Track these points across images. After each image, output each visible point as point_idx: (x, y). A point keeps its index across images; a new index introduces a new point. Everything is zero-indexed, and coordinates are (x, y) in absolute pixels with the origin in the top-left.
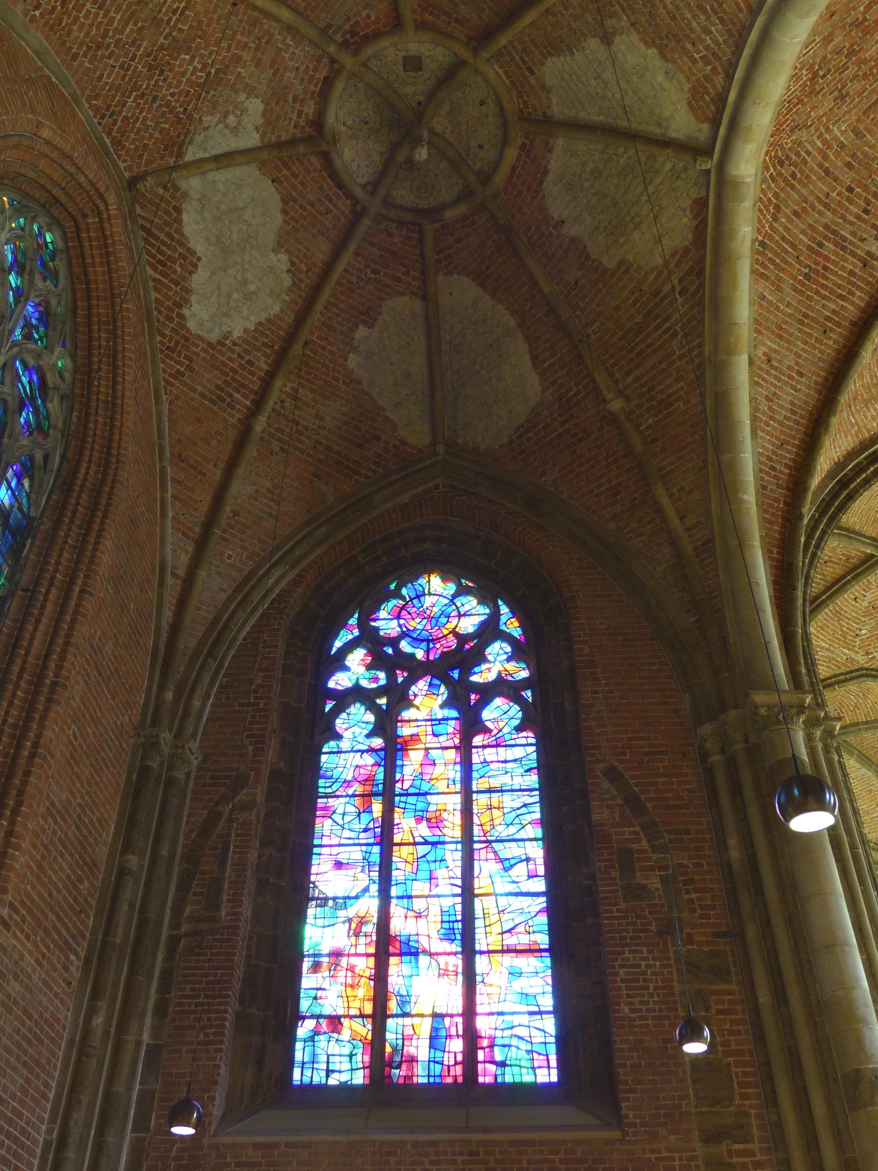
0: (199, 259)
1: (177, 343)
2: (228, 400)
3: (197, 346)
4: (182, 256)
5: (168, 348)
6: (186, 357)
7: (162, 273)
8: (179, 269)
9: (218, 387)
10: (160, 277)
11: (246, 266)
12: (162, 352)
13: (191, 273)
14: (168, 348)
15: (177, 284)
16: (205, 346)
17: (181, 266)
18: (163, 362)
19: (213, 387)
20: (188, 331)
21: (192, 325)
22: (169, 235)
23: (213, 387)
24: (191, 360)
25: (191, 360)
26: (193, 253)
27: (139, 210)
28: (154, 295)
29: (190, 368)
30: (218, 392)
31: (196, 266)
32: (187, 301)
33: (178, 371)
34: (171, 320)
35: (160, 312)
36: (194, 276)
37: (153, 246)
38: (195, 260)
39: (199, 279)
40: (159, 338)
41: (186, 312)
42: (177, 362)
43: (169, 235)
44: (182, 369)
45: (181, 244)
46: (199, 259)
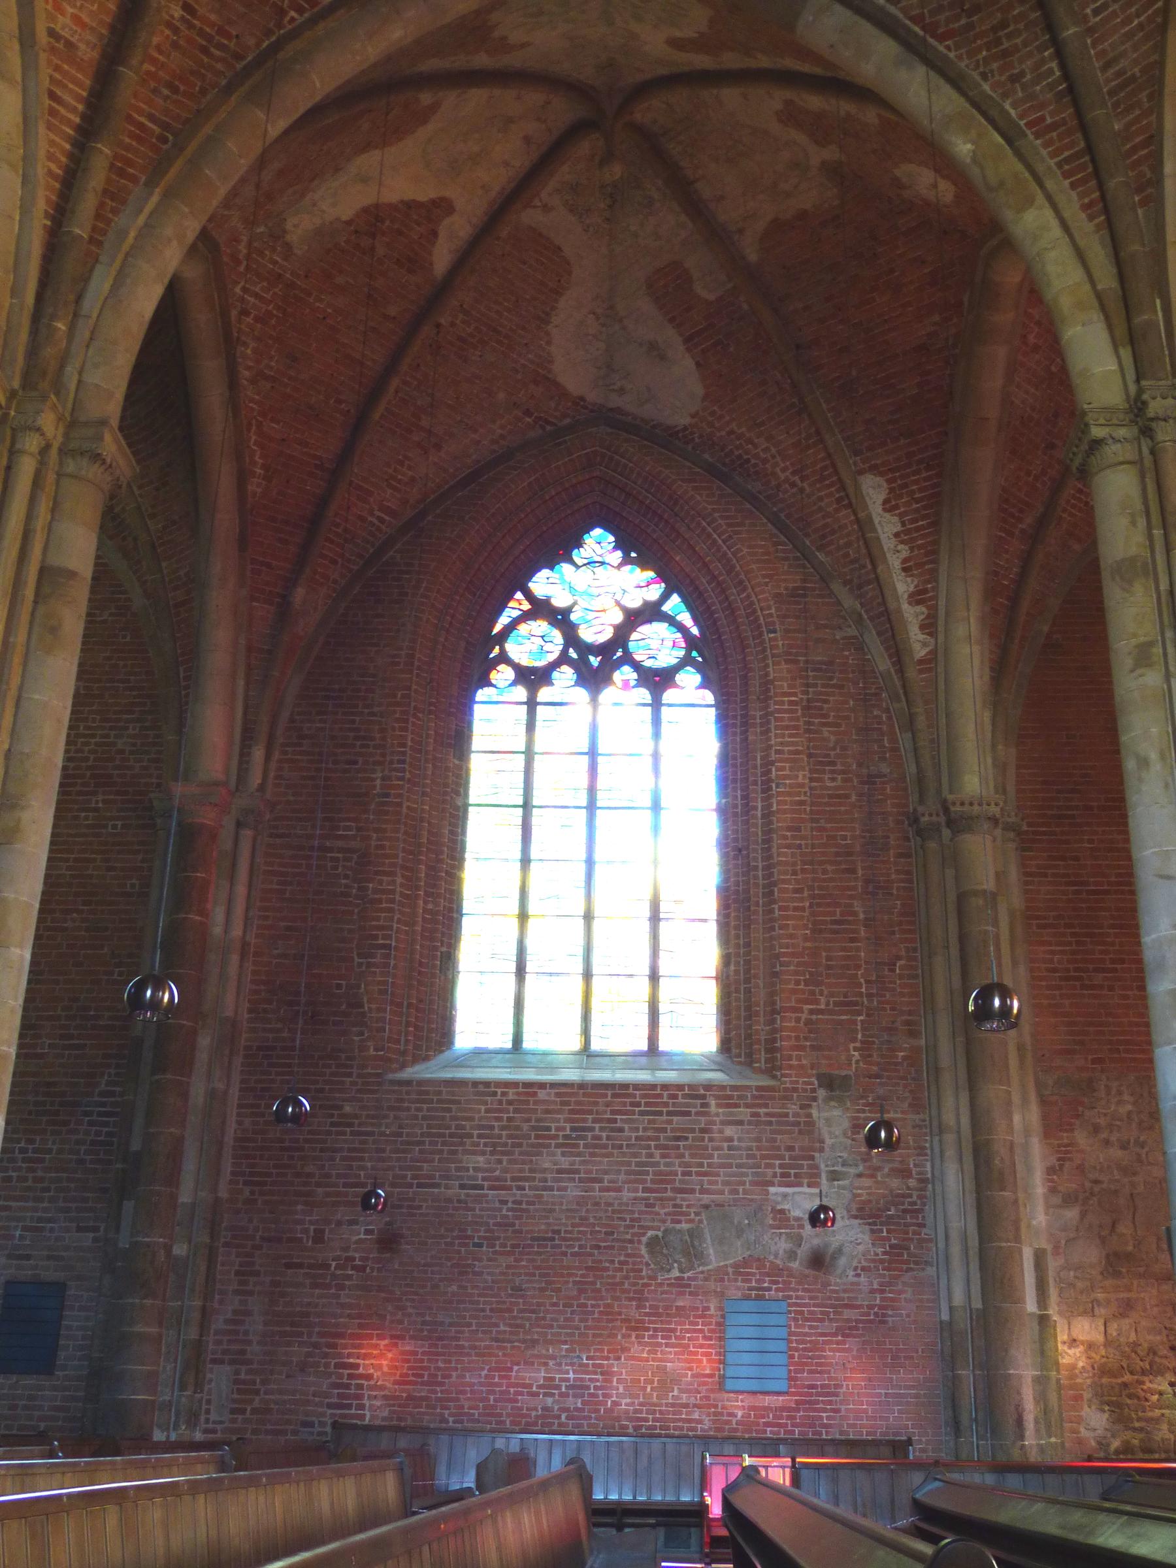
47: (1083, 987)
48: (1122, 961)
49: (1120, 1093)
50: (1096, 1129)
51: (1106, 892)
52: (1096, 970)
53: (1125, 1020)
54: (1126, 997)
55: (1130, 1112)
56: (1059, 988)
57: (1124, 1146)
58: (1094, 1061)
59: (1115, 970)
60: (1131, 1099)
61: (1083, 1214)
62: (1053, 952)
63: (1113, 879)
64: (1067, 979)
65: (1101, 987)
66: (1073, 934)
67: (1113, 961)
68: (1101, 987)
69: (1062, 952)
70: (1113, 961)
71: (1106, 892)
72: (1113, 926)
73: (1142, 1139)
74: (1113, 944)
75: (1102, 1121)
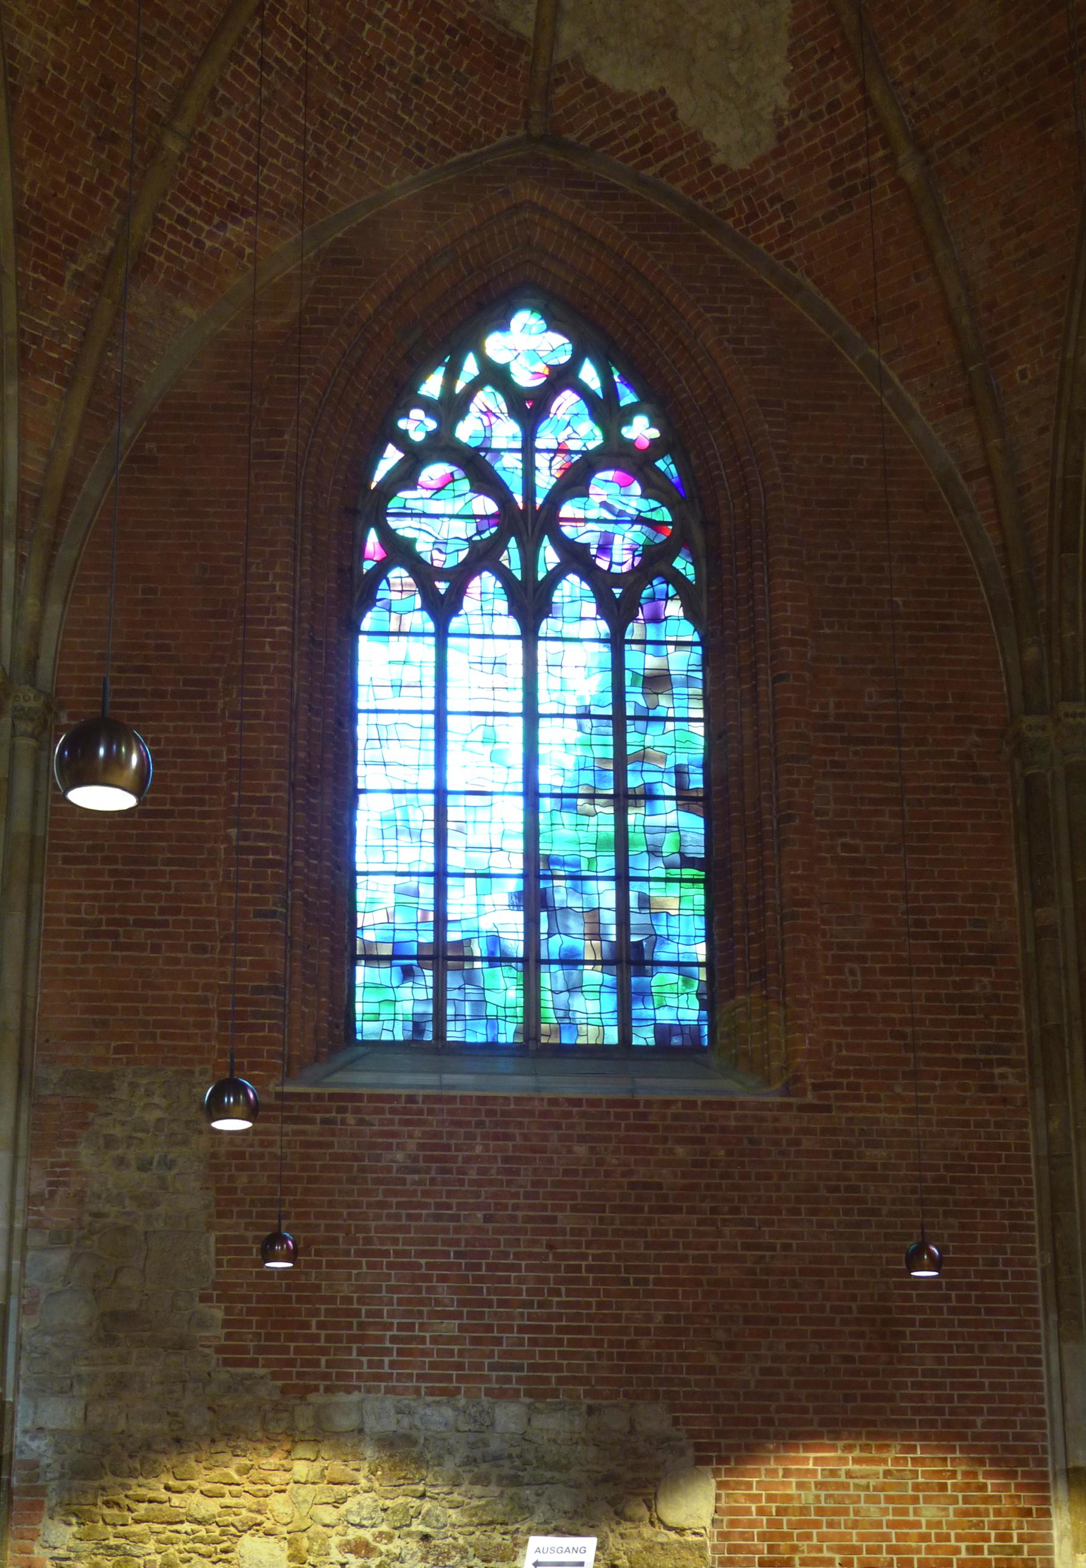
0: (663, 91)
1: (748, 200)
2: (858, 181)
3: (766, 175)
4: (651, 113)
5: (749, 218)
6: (772, 202)
7: (659, 157)
8: (660, 132)
9: (833, 184)
10: (662, 163)
11: (704, 20)
12: (746, 231)
13: (674, 117)
14: (749, 218)
15: (678, 146)
16: (774, 163)
17: (660, 124)
18: (758, 240)
19: (830, 192)
20: (743, 172)
21: (739, 163)
22: (618, 114)
23: (830, 192)
24: (778, 198)
25: (778, 198)
26: (650, 96)
27: (572, 137)
28: (678, 187)
29: (789, 208)
30: (840, 189)
31: (669, 103)
32: (706, 147)
33: (782, 228)
34: (716, 188)
35: (701, 195)
36: (680, 113)
37: (620, 147)
38: (661, 99)
39: (689, 109)
40: (730, 222)
41: (718, 159)
42: (770, 221)
43: (618, 114)
44: (782, 220)
45: (633, 106)
46: (663, 91)
47: (118, 946)
48: (177, 911)
49: (149, 1094)
50: (110, 1142)
51: (169, 814)
52: (138, 923)
53: (170, 993)
54: (176, 962)
55: (159, 1120)
56: (82, 947)
57: (144, 1166)
58: (117, 1050)
59: (165, 924)
60: (164, 1103)
61: (75, 1259)
62: (80, 897)
63: (180, 795)
64: (97, 934)
65: (141, 947)
66: (114, 873)
67: (163, 911)
68: (141, 947)
69: (95, 898)
70: (163, 911)
71: (169, 814)
72: (169, 862)
73: (170, 1156)
74: (167, 887)
75: (118, 1131)
